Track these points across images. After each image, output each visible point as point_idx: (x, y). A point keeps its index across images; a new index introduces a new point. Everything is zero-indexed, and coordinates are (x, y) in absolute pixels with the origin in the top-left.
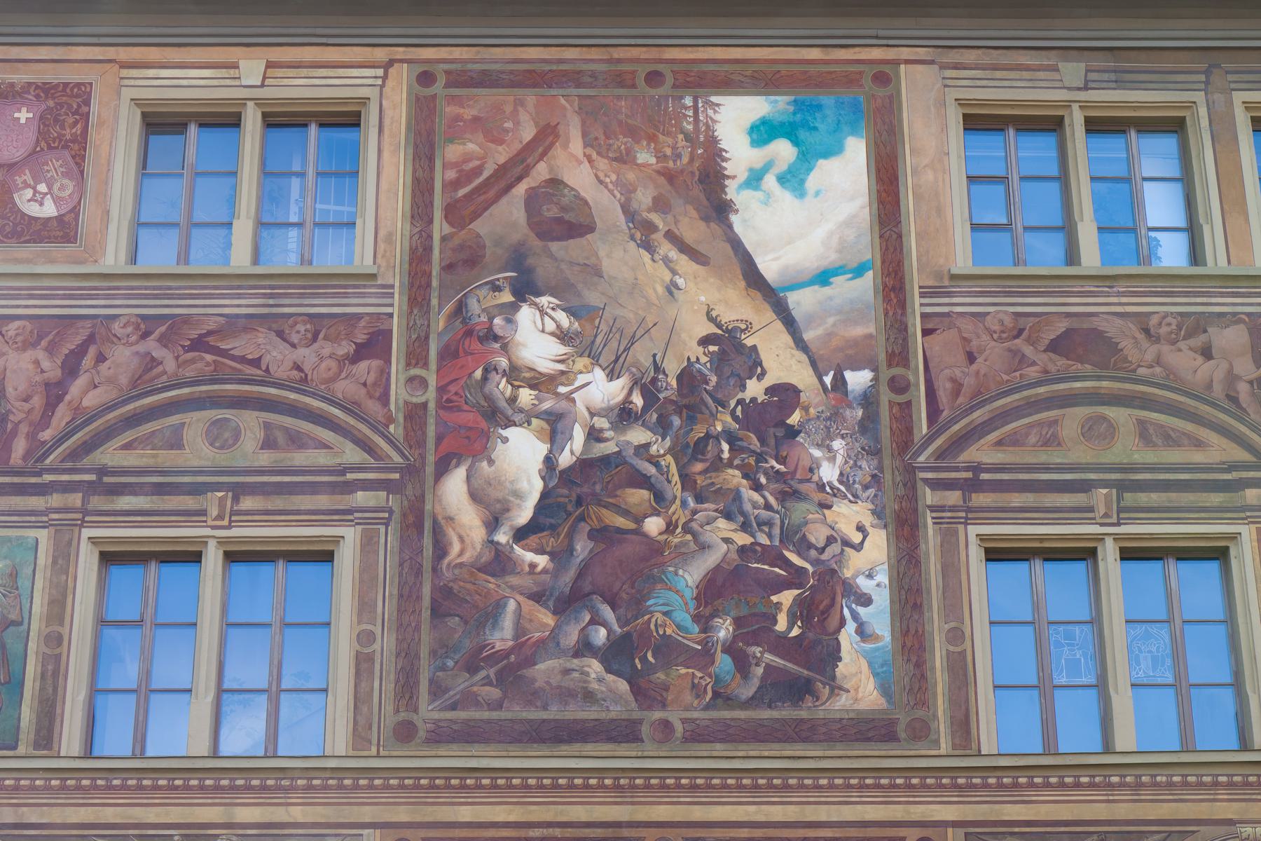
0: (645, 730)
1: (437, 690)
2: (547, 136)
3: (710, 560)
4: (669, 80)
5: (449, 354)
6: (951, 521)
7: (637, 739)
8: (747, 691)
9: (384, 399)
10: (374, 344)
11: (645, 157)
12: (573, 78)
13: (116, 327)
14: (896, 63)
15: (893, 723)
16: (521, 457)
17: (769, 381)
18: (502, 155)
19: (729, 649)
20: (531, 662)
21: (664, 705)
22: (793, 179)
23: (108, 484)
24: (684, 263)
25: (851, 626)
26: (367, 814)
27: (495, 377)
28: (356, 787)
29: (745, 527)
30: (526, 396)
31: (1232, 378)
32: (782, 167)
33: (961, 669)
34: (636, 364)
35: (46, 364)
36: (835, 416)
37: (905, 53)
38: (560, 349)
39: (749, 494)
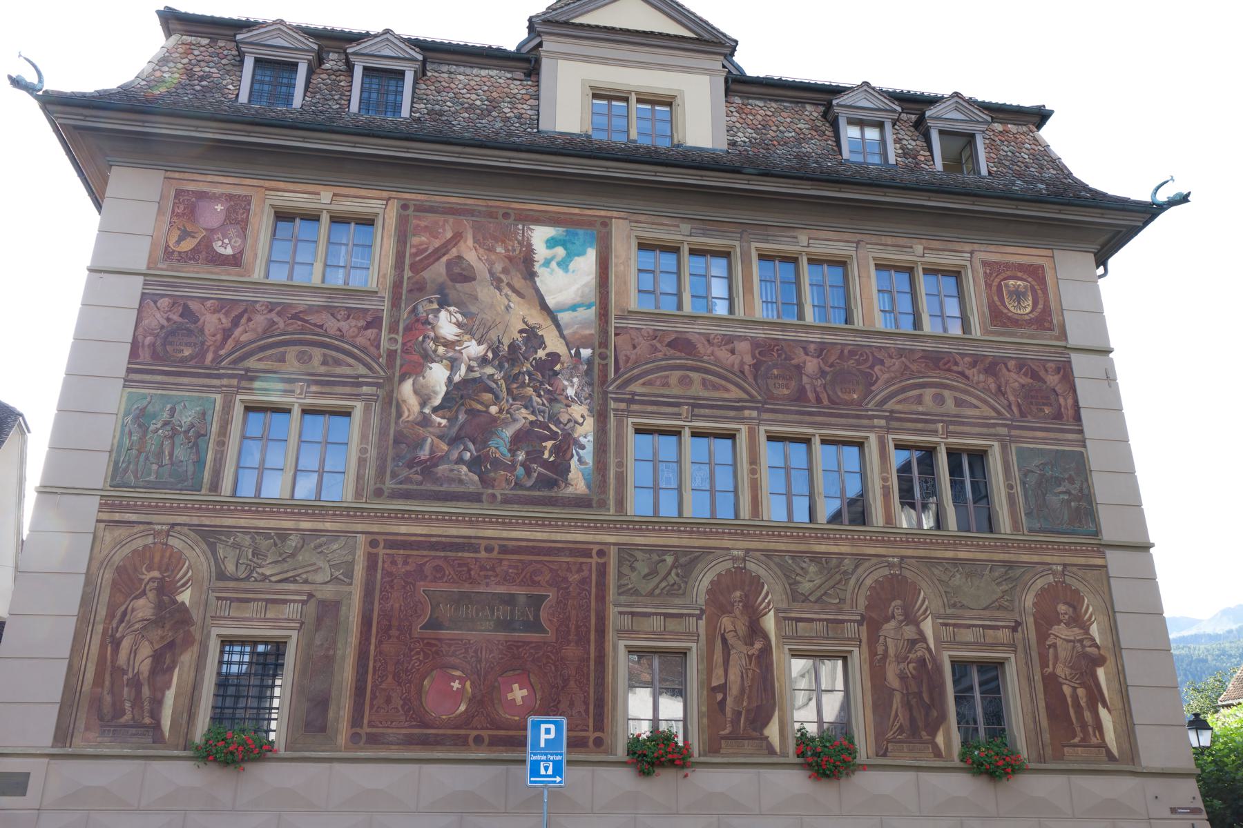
0: (484, 497)
1: (394, 475)
2: (457, 237)
3: (517, 426)
4: (513, 217)
5: (408, 329)
6: (621, 416)
7: (481, 501)
8: (529, 483)
9: (378, 347)
10: (375, 323)
11: (500, 249)
12: (470, 212)
13: (258, 306)
14: (611, 218)
15: (591, 500)
16: (438, 376)
17: (547, 351)
18: (437, 243)
19: (523, 465)
20: (436, 465)
21: (493, 487)
22: (564, 264)
24: (514, 297)
25: (576, 458)
26: (359, 528)
27: (428, 341)
28: (355, 516)
29: (533, 413)
30: (441, 350)
31: (742, 363)
32: (559, 259)
33: (621, 479)
34: (491, 339)
35: (224, 320)
36: (575, 367)
37: (615, 214)
38: (457, 330)
39: (536, 399)
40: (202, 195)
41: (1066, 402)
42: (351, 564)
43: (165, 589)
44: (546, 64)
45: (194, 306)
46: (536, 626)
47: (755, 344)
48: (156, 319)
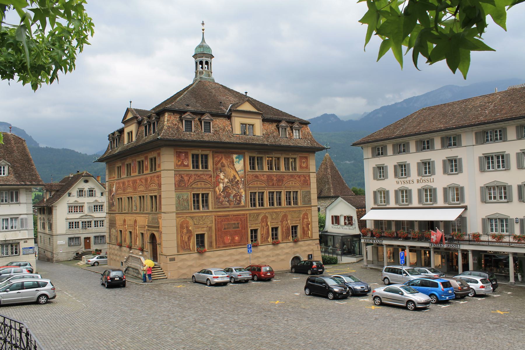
2: (222, 158)
10: (211, 177)
16: (221, 186)
22: (238, 162)
23: (193, 189)
40: (180, 152)
41: (309, 182)
42: (212, 221)
43: (187, 227)
44: (233, 118)
45: (183, 175)
46: (238, 227)
47: (267, 175)
48: (177, 179)
